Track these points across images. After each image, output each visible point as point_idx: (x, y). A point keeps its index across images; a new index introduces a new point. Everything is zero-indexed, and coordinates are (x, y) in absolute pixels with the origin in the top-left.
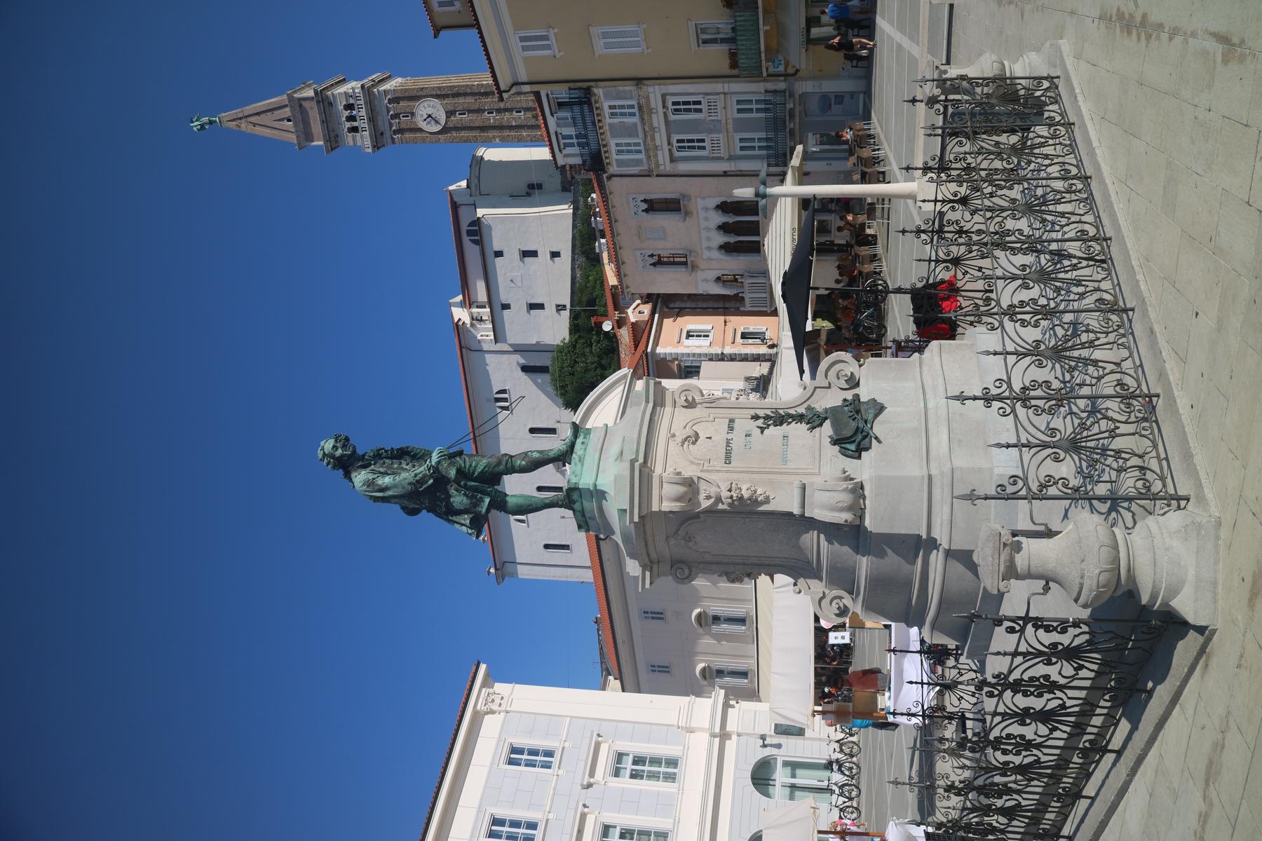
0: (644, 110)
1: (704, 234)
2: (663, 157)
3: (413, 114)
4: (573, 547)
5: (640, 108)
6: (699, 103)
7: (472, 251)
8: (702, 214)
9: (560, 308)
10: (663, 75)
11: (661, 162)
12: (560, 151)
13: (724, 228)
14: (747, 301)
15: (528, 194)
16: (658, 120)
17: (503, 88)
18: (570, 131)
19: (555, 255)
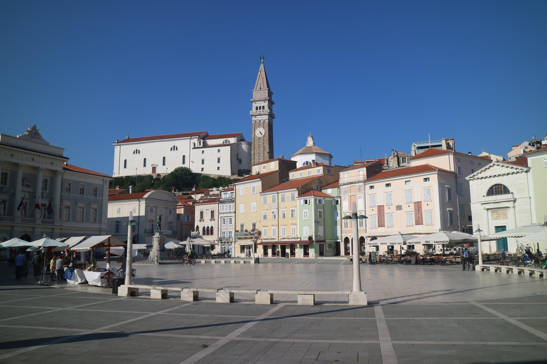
0: (230, 213)
1: (207, 223)
2: (222, 215)
3: (261, 127)
4: (125, 169)
5: (230, 212)
6: (231, 224)
7: (220, 141)
8: (211, 223)
9: (202, 169)
10: (236, 217)
11: (221, 215)
12: (224, 193)
13: (208, 227)
14: (193, 232)
15: (238, 159)
16: (228, 215)
17: (235, 184)
18: (227, 197)
19: (218, 168)
